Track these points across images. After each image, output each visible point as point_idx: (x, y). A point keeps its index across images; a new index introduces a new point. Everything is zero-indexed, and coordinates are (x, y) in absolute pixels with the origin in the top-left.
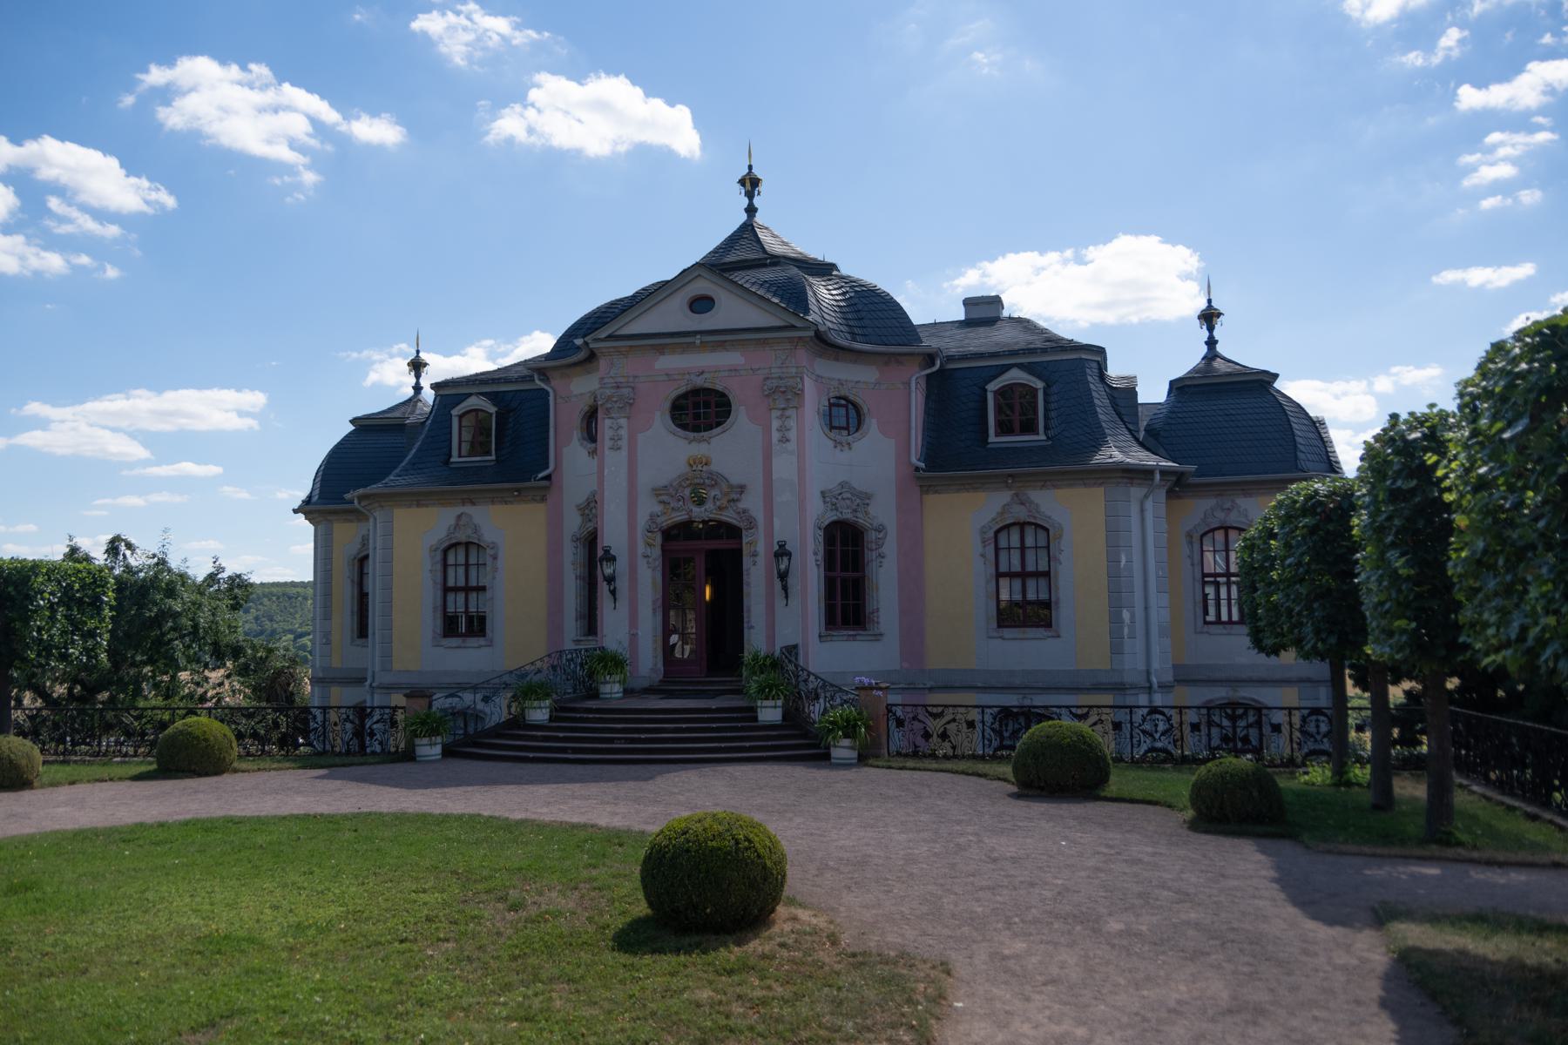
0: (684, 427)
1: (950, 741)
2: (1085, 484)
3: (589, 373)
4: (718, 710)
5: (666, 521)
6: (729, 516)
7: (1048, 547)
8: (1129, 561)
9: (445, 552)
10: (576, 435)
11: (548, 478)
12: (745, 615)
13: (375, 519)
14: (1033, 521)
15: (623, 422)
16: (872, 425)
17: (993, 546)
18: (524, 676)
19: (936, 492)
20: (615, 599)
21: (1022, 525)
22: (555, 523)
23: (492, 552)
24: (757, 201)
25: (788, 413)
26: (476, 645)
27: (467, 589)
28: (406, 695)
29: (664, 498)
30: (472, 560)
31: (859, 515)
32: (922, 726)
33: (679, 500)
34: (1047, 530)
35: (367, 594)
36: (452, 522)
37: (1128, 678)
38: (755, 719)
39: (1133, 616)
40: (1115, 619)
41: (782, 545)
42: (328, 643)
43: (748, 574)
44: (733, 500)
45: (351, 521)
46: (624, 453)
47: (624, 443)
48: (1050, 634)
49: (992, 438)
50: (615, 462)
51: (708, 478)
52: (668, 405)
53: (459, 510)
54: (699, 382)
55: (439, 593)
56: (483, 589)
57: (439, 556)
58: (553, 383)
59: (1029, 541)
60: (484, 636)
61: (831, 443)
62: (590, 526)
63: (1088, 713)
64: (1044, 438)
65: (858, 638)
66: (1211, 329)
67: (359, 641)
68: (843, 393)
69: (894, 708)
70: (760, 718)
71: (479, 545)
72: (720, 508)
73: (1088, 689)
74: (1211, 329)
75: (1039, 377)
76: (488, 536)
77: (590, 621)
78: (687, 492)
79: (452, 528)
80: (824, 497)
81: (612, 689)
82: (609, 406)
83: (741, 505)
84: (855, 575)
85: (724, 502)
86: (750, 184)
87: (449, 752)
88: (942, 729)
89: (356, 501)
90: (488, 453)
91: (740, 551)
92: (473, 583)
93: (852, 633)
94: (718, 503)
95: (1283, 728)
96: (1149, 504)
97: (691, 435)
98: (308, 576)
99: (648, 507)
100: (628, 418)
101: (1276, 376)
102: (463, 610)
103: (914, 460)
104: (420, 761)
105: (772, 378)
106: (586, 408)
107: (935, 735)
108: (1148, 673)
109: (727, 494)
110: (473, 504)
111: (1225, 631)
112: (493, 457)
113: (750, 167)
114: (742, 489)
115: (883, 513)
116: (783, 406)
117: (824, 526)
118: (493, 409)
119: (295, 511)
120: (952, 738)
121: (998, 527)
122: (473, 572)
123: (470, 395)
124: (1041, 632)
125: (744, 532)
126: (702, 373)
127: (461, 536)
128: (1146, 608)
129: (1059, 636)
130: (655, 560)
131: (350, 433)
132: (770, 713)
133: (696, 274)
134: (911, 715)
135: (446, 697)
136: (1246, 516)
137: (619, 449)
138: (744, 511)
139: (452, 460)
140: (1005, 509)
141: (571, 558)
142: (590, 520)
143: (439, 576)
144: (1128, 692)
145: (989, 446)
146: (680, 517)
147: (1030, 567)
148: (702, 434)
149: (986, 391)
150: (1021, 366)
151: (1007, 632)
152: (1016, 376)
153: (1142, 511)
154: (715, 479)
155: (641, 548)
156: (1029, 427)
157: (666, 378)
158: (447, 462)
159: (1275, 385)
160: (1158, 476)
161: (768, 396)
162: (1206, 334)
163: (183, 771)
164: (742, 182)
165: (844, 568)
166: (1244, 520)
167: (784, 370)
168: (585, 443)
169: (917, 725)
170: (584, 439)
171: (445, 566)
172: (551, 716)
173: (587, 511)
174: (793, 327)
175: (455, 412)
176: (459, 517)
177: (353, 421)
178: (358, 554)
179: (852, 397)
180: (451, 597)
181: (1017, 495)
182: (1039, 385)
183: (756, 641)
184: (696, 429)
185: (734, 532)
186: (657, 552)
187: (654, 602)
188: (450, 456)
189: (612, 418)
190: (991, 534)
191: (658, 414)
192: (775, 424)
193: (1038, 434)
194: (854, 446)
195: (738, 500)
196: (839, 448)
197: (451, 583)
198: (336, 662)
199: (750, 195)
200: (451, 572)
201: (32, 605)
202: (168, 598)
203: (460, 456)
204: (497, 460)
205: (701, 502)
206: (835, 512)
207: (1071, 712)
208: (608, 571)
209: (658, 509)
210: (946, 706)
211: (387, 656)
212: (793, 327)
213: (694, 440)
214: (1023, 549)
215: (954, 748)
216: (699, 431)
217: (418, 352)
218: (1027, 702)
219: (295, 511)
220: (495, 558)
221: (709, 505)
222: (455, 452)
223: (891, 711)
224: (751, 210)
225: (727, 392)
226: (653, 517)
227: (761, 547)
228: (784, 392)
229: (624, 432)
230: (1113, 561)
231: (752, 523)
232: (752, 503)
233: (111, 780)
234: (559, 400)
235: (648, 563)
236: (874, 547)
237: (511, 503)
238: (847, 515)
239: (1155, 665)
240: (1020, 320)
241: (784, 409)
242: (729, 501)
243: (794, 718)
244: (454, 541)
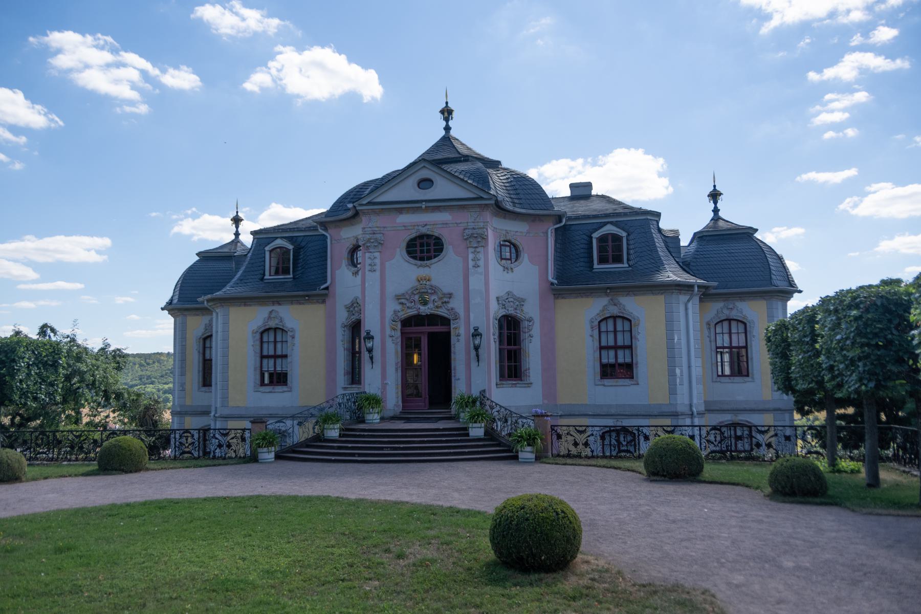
0: (415, 258)
1: (590, 448)
2: (653, 293)
3: (353, 225)
4: (444, 430)
5: (403, 315)
6: (442, 312)
7: (631, 331)
8: (679, 339)
9: (262, 333)
10: (344, 262)
11: (327, 288)
12: (453, 372)
13: (217, 314)
14: (621, 315)
15: (377, 254)
16: (525, 257)
17: (598, 330)
18: (322, 410)
19: (563, 298)
20: (372, 362)
21: (615, 318)
22: (331, 317)
24: (451, 123)
25: (478, 250)
26: (281, 391)
27: (275, 357)
28: (251, 422)
29: (403, 301)
30: (279, 339)
31: (518, 311)
32: (573, 438)
33: (412, 302)
34: (630, 321)
35: (211, 360)
36: (266, 315)
37: (680, 409)
38: (468, 435)
39: (682, 372)
40: (672, 374)
41: (476, 329)
42: (184, 390)
43: (454, 347)
44: (445, 302)
45: (198, 315)
46: (378, 273)
47: (378, 267)
48: (633, 383)
49: (596, 266)
50: (373, 279)
51: (430, 289)
52: (404, 245)
53: (270, 308)
54: (424, 230)
55: (258, 359)
56: (286, 356)
57: (258, 336)
58: (329, 231)
59: (619, 328)
60: (286, 385)
61: (502, 268)
62: (354, 318)
63: (674, 430)
64: (627, 266)
65: (518, 385)
66: (715, 203)
67: (204, 389)
68: (508, 238)
69: (555, 428)
70: (470, 435)
71: (283, 330)
72: (437, 307)
73: (656, 416)
74: (715, 203)
75: (623, 229)
76: (289, 324)
77: (355, 376)
78: (417, 297)
79: (266, 319)
80: (498, 301)
81: (373, 418)
82: (369, 245)
83: (450, 306)
84: (515, 347)
85: (439, 303)
86: (447, 113)
87: (278, 457)
88: (585, 440)
89: (205, 302)
90: (289, 273)
91: (448, 334)
92: (279, 352)
93: (514, 382)
94: (436, 304)
95: (792, 438)
96: (690, 305)
97: (419, 263)
98: (168, 347)
99: (392, 306)
100: (380, 252)
101: (756, 230)
102: (273, 369)
103: (550, 279)
104: (261, 463)
105: (469, 229)
106: (351, 246)
107: (581, 444)
108: (691, 406)
109: (441, 298)
110: (280, 304)
111: (730, 381)
112: (291, 276)
113: (447, 103)
114: (450, 295)
115: (531, 311)
116: (475, 245)
117: (498, 318)
118: (291, 247)
119: (163, 309)
120: (591, 446)
121: (601, 319)
122: (279, 346)
123: (277, 238)
124: (627, 381)
125: (452, 321)
126: (426, 225)
127: (272, 324)
128: (689, 367)
129: (638, 384)
130: (397, 338)
131: (197, 261)
132: (477, 431)
133: (422, 165)
134: (566, 432)
135: (276, 422)
136: (742, 313)
137: (374, 271)
138: (452, 309)
139: (265, 277)
140: (605, 308)
141: (341, 338)
142: (354, 315)
143: (258, 348)
144: (680, 417)
145: (594, 271)
146: (412, 312)
147: (620, 343)
148: (426, 262)
149: (591, 238)
150: (611, 223)
151: (607, 382)
152: (609, 229)
153: (686, 309)
154: (434, 290)
155: (388, 331)
156: (618, 259)
157: (403, 228)
158: (262, 279)
159: (755, 235)
160: (696, 289)
161: (466, 239)
162: (712, 206)
163: (116, 470)
164: (442, 112)
165: (509, 344)
166: (740, 315)
167: (476, 224)
168: (350, 267)
169: (569, 438)
170: (349, 265)
171: (262, 342)
172: (340, 434)
173: (351, 309)
174: (481, 198)
175: (267, 248)
176: (271, 312)
177: (197, 254)
178: (203, 335)
179: (513, 241)
180: (265, 361)
181: (612, 300)
182: (624, 234)
183: (459, 388)
184: (422, 259)
185: (446, 321)
186: (399, 333)
188: (264, 275)
189: (371, 252)
190: (596, 323)
191: (398, 250)
192: (471, 256)
193: (623, 263)
194: (514, 269)
195: (448, 302)
196: (506, 271)
197: (265, 353)
198: (188, 402)
199: (447, 120)
200: (265, 346)
201: (17, 366)
202: (78, 362)
203: (270, 275)
204: (294, 278)
205: (425, 303)
206: (504, 310)
207: (664, 430)
208: (369, 345)
209: (399, 307)
210: (588, 426)
211: (225, 398)
212: (481, 198)
213: (421, 266)
214: (615, 332)
215: (592, 451)
216: (424, 260)
217: (237, 212)
218: (619, 424)
219: (163, 309)
220: (293, 337)
221: (431, 305)
222: (267, 273)
223: (554, 430)
224: (447, 129)
225: (441, 237)
226: (395, 312)
227: (462, 331)
228: (476, 237)
229: (378, 261)
230: (670, 339)
231: (457, 318)
232: (457, 304)
233: (70, 476)
234: (333, 242)
235: (393, 340)
236: (527, 330)
237: (303, 304)
238: (511, 311)
239: (695, 401)
240: (603, 197)
241: (476, 247)
242: (443, 303)
243: (490, 434)
244: (267, 327)
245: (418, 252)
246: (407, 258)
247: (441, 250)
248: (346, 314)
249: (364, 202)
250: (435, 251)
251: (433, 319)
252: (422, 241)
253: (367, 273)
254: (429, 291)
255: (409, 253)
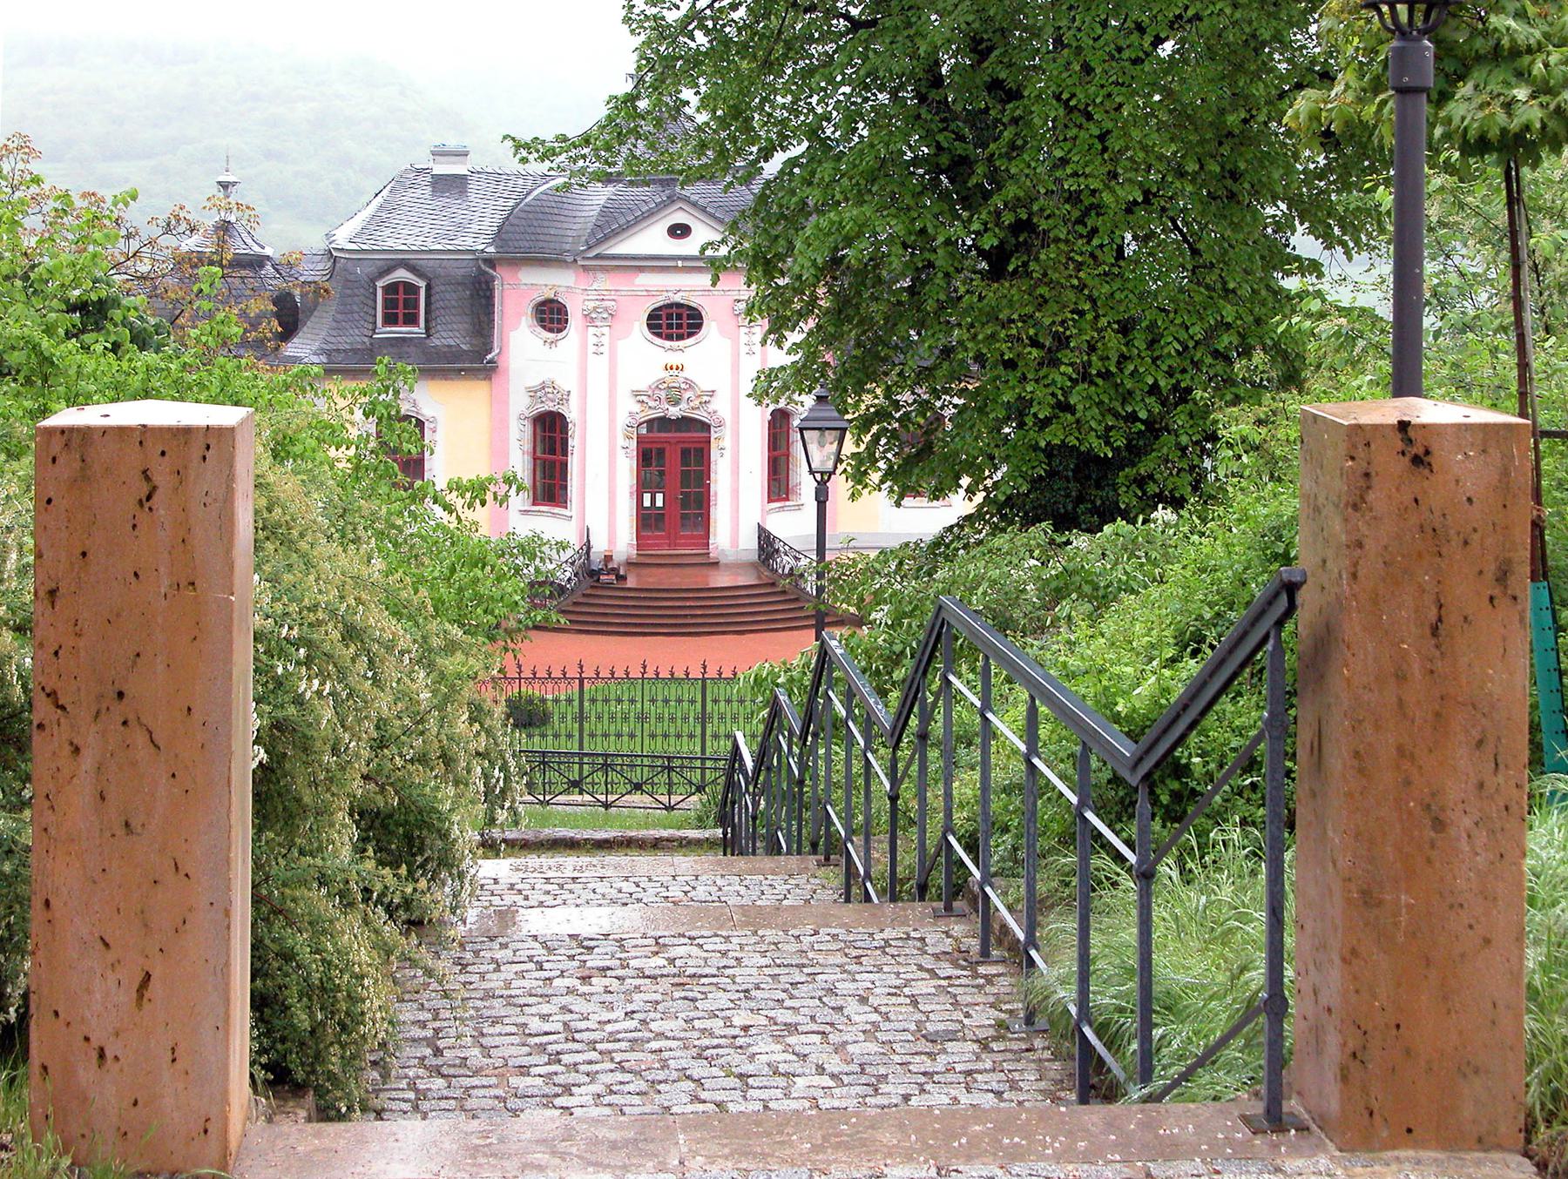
0: (659, 335)
6: (700, 415)
15: (605, 330)
23: (432, 426)
25: (753, 330)
29: (644, 398)
46: (605, 357)
54: (677, 298)
78: (663, 394)
82: (594, 315)
154: (690, 385)
173: (539, 394)
175: (380, 284)
185: (706, 427)
187: (631, 487)
192: (744, 339)
205: (676, 403)
209: (637, 408)
221: (683, 405)
229: (605, 340)
245: (664, 327)
246: (650, 336)
247: (699, 326)
248: (527, 401)
249: (591, 255)
250: (690, 326)
251: (686, 423)
252: (670, 311)
253: (591, 357)
254: (683, 386)
255: (650, 326)
